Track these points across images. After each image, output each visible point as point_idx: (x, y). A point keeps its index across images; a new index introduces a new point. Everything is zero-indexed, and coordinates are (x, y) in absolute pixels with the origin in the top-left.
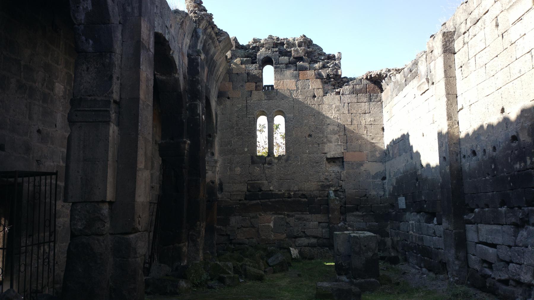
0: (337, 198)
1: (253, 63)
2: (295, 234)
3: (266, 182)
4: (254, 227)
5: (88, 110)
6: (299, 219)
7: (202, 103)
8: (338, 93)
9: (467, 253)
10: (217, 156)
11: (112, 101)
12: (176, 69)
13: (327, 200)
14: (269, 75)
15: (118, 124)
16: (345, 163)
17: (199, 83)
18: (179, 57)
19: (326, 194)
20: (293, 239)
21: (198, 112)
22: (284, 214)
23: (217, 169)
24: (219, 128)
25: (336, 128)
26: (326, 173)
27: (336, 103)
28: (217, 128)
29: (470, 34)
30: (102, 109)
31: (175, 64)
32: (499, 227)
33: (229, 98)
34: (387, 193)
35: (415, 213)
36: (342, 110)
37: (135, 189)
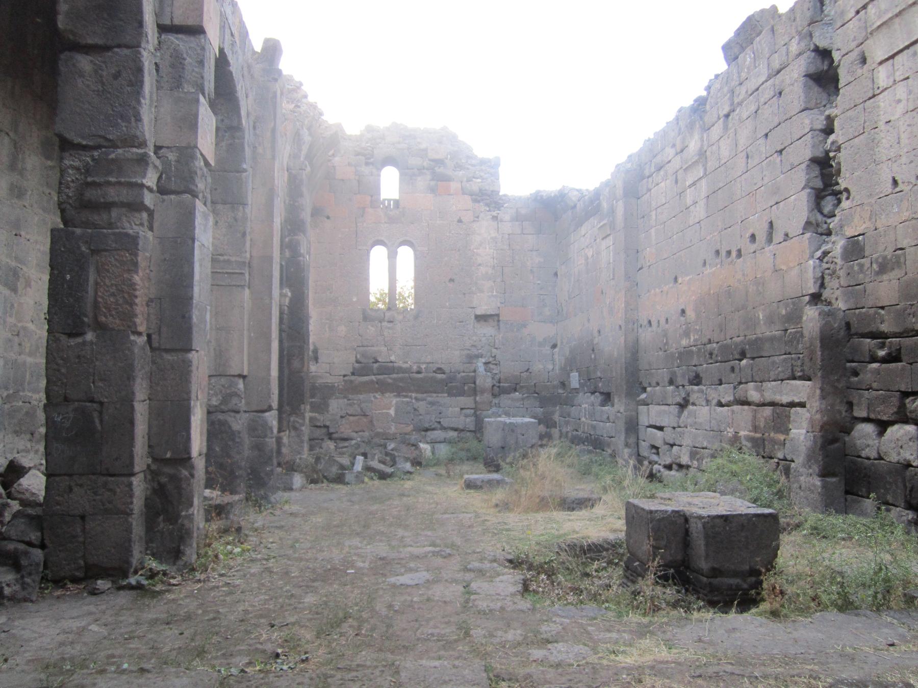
1: (367, 164)
2: (427, 425)
3: (384, 349)
4: (365, 416)
6: (432, 404)
8: (495, 218)
13: (475, 377)
16: (502, 325)
19: (472, 369)
20: (423, 433)
21: (302, 251)
22: (411, 397)
25: (490, 271)
26: (474, 338)
32: (666, 408)
33: (328, 218)
34: (557, 367)
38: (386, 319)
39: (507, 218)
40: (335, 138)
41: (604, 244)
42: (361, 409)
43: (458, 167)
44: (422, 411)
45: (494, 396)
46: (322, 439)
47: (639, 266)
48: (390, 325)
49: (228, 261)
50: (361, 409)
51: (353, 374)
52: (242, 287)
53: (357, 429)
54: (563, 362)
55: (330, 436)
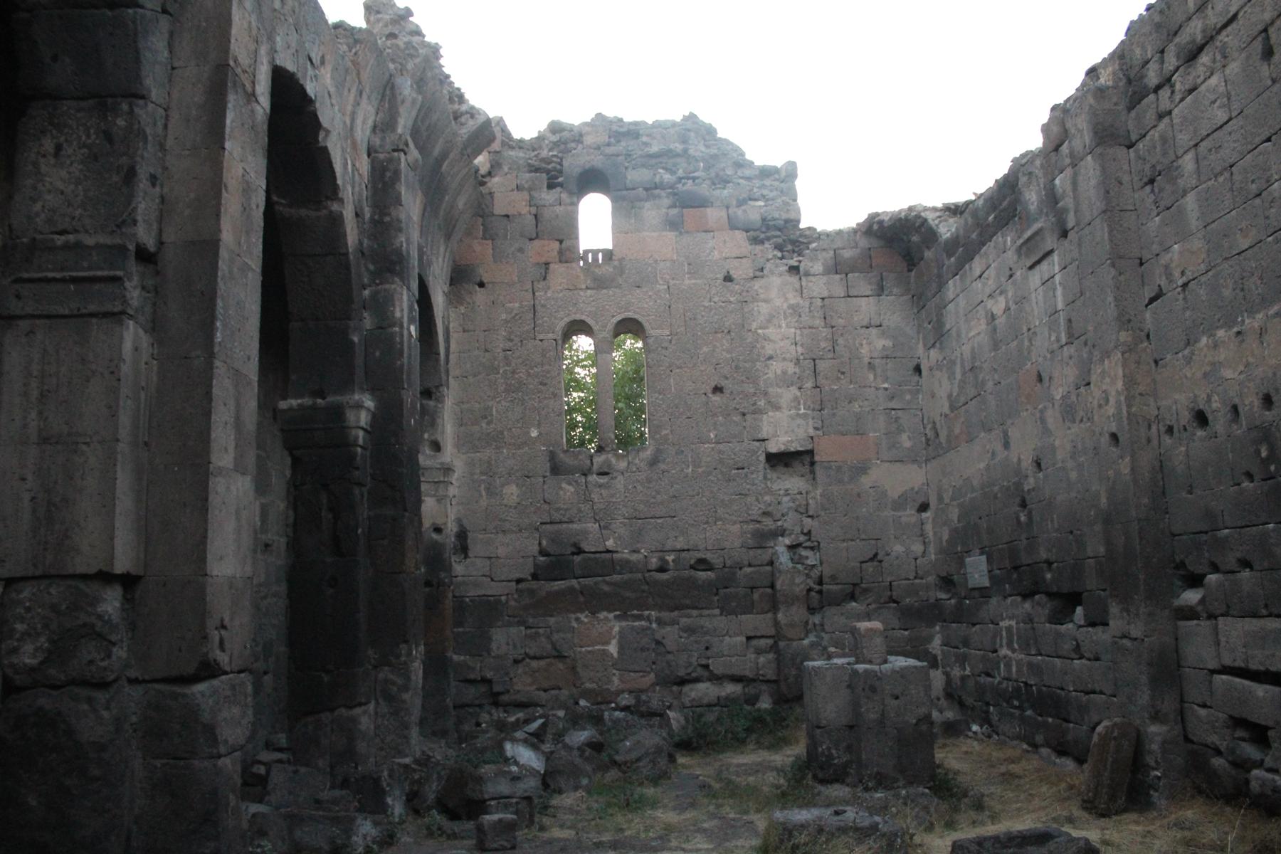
0: (799, 566)
2: (682, 673)
4: (561, 657)
5: (54, 280)
6: (690, 630)
7: (408, 289)
8: (794, 270)
9: (1182, 701)
10: (449, 453)
11: (132, 247)
12: (335, 188)
13: (773, 574)
14: (595, 222)
15: (155, 327)
16: (817, 467)
17: (400, 230)
18: (343, 150)
20: (675, 688)
21: (398, 314)
22: (648, 619)
23: (452, 491)
24: (454, 371)
25: (791, 369)
26: (767, 498)
27: (790, 296)
28: (447, 371)
29: (1178, 86)
30: (99, 273)
31: (333, 172)
33: (481, 285)
35: (1019, 599)
36: (804, 318)
37: (205, 537)
38: (595, 467)
39: (818, 267)
40: (488, 133)
41: (1035, 278)
42: (554, 645)
43: (721, 181)
44: (670, 644)
45: (812, 610)
46: (480, 706)
47: (1148, 293)
48: (603, 480)
49: (78, 245)
50: (554, 645)
51: (535, 577)
52: (117, 317)
53: (546, 685)
54: (946, 537)
55: (495, 700)
